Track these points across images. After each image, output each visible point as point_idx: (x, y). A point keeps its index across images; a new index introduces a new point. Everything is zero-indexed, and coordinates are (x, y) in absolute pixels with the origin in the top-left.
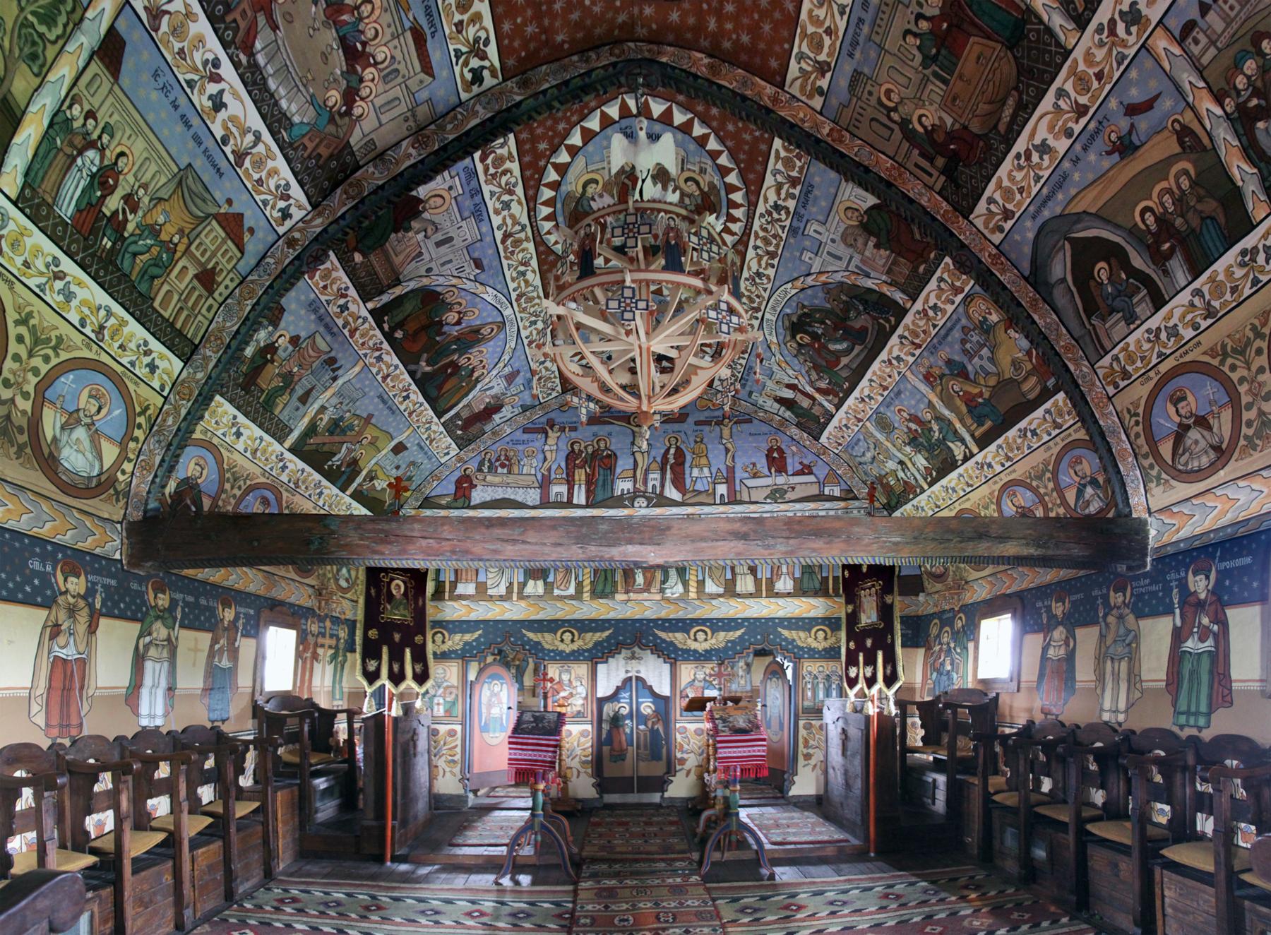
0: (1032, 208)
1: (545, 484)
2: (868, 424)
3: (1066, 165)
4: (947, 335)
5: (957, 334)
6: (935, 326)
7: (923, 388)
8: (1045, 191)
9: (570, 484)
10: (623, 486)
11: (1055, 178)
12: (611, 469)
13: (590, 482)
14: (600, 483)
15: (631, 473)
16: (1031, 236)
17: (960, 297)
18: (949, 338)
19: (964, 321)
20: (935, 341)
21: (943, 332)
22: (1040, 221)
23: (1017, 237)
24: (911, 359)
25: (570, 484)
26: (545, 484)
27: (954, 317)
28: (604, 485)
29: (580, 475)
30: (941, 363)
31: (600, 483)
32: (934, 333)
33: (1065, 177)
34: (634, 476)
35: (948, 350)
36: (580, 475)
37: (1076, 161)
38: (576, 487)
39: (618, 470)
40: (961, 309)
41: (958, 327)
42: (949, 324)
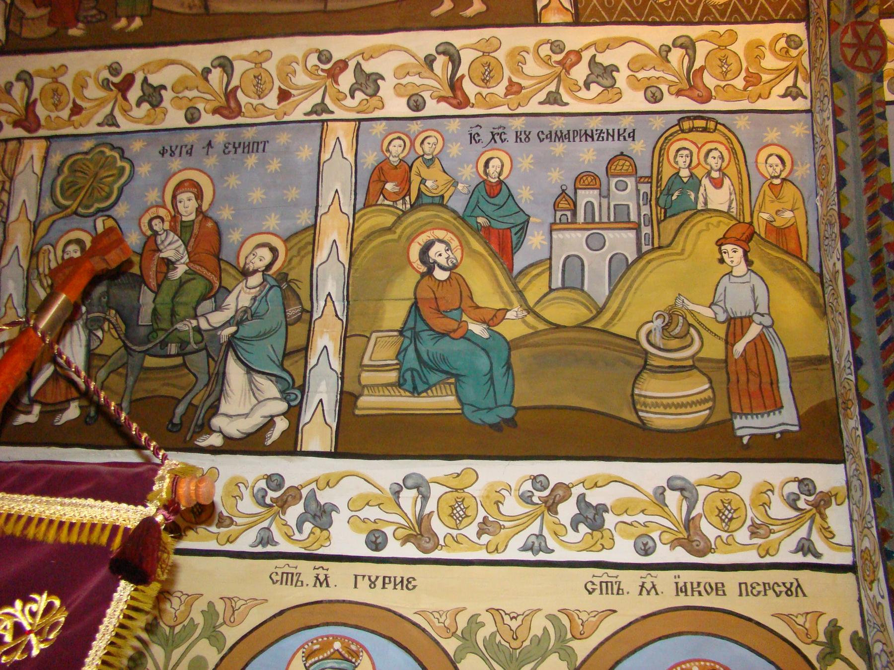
2: (35, 149)
4: (561, 136)
5: (590, 156)
6: (554, 98)
7: (338, 181)
17: (686, 104)
18: (559, 148)
19: (639, 148)
20: (518, 124)
21: (559, 124)
24: (397, 107)
27: (626, 122)
30: (468, 175)
32: (533, 107)
35: (525, 163)
40: (659, 124)
41: (613, 147)
42: (594, 124)
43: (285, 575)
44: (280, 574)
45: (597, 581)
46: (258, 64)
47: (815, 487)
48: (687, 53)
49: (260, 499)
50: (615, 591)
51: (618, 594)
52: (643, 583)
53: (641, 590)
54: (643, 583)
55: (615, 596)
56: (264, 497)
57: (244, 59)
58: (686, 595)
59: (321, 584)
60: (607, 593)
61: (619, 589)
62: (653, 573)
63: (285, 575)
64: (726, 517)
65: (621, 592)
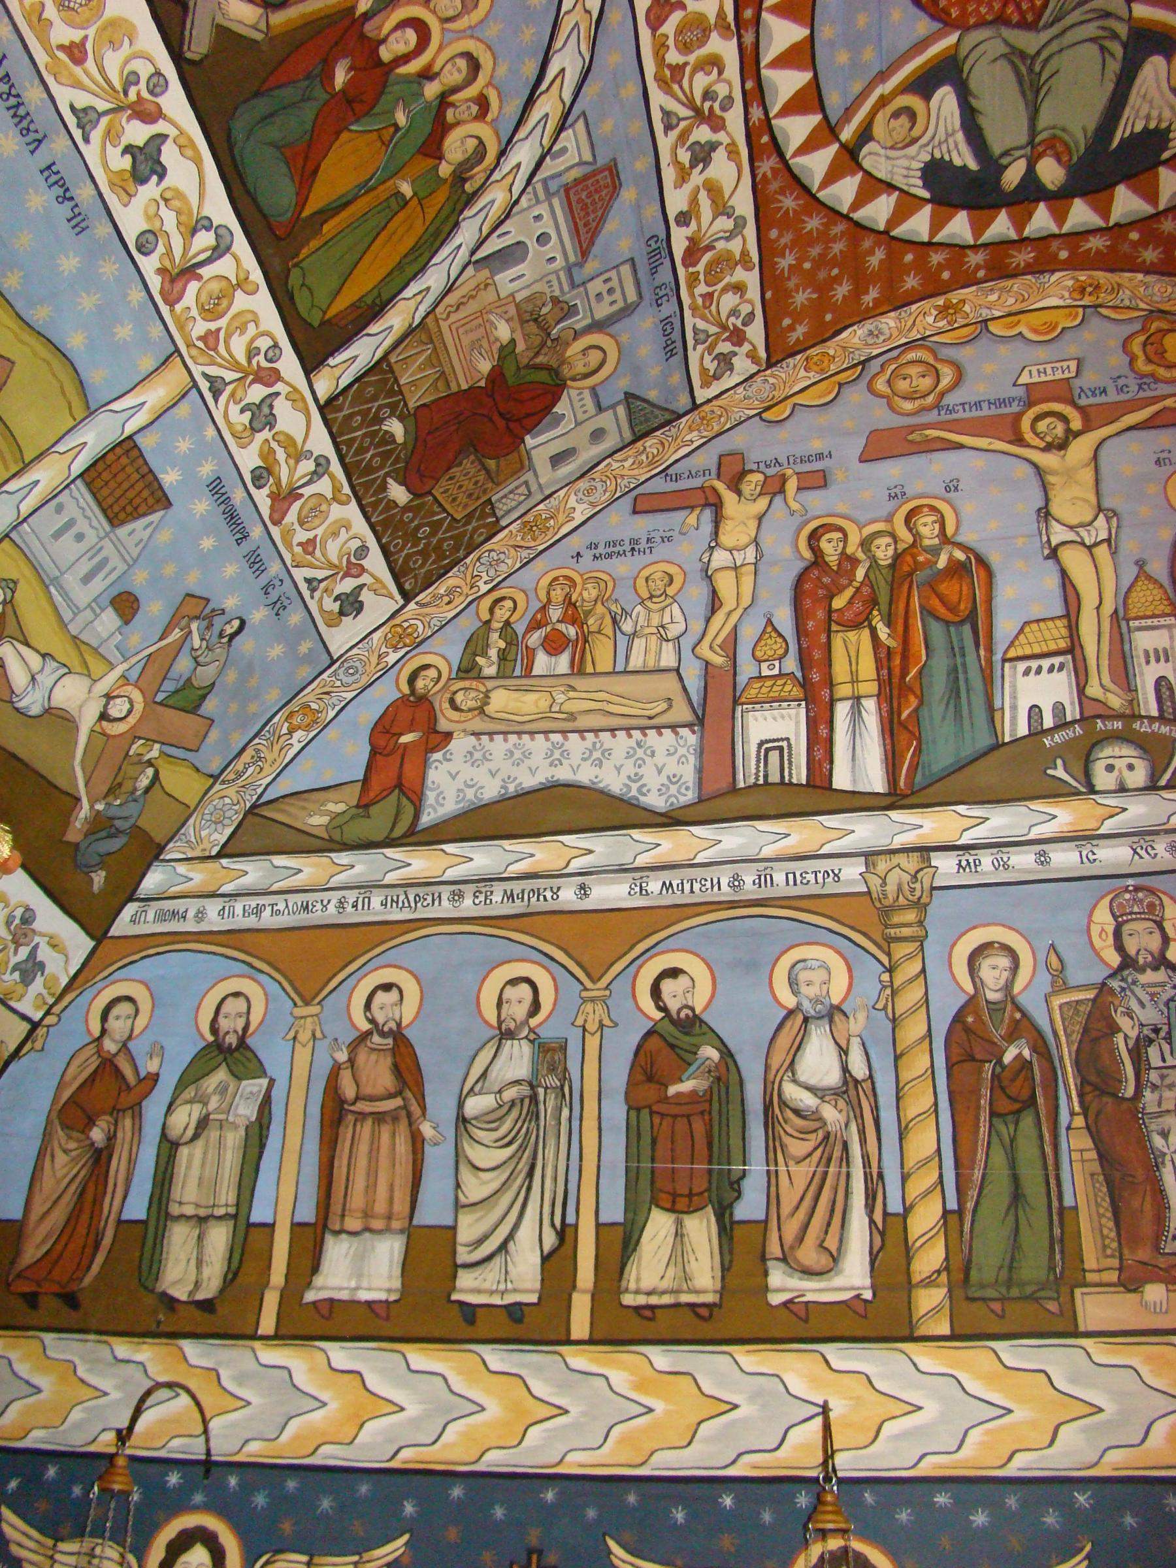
1: (714, 709)
9: (817, 696)
10: (1036, 693)
12: (975, 619)
13: (895, 687)
14: (938, 685)
15: (1056, 636)
25: (817, 696)
26: (714, 709)
28: (954, 692)
29: (854, 657)
31: (938, 685)
34: (1074, 648)
36: (854, 657)
38: (842, 711)
39: (1005, 626)
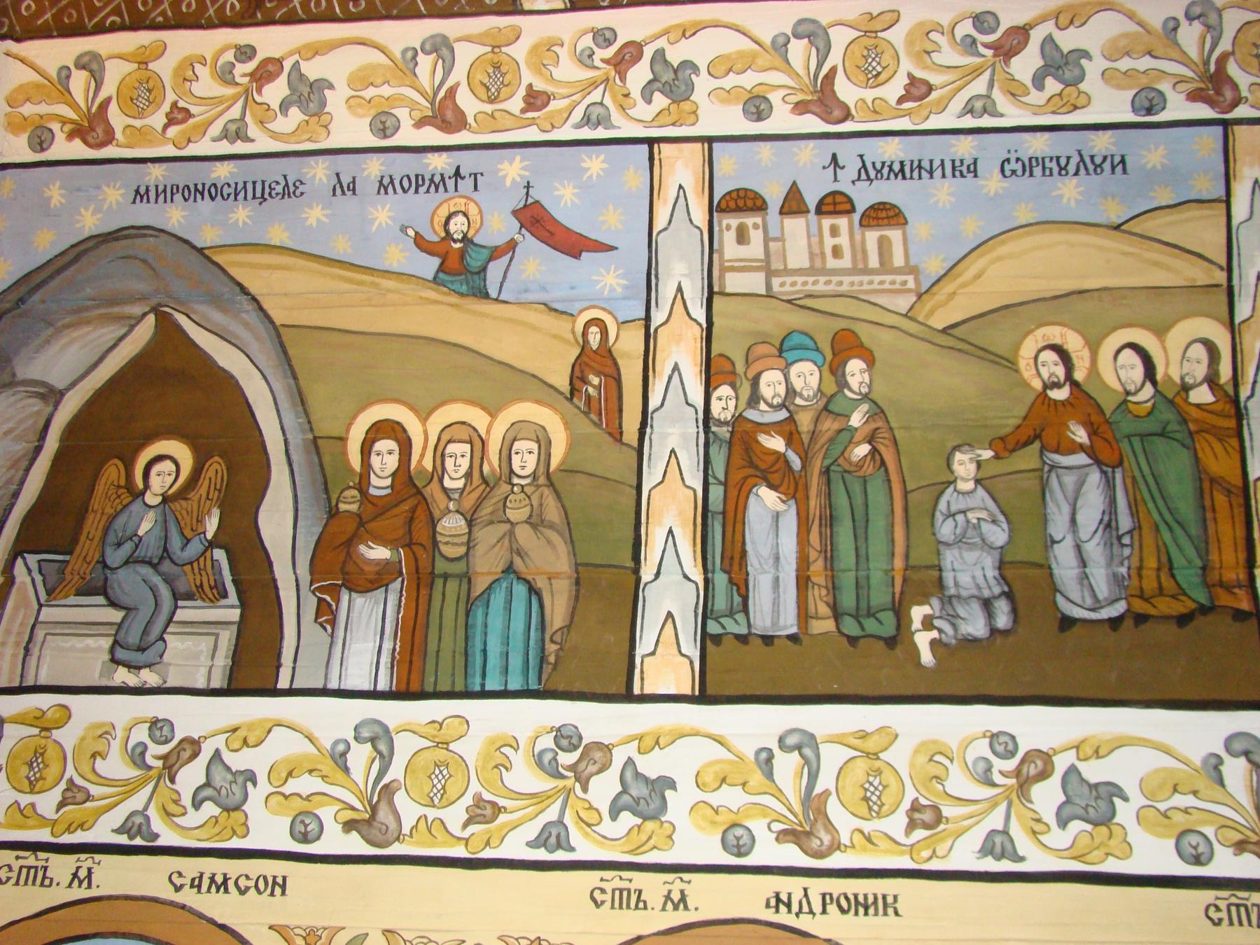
0: (156, 173)
3: (319, 171)
8: (222, 172)
11: (271, 171)
16: (90, 223)
22: (145, 215)
23: (56, 195)
33: (290, 190)
37: (345, 187)
43: (24, 871)
44: (16, 869)
45: (609, 889)
46: (144, 64)
47: (581, 738)
48: (439, 57)
49: (137, 756)
50: (633, 904)
51: (637, 907)
52: (670, 892)
53: (665, 904)
54: (670, 892)
55: (37, 888)
56: (143, 754)
57: (120, 57)
58: (199, 891)
59: (81, 883)
60: (621, 907)
61: (44, 877)
62: (686, 876)
63: (24, 871)
64: (876, 789)
65: (641, 905)
